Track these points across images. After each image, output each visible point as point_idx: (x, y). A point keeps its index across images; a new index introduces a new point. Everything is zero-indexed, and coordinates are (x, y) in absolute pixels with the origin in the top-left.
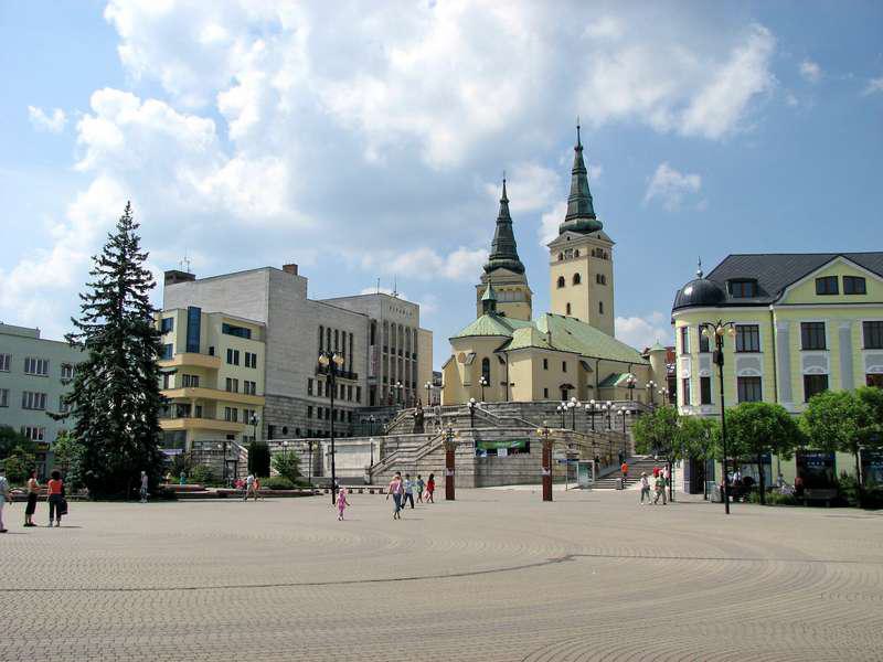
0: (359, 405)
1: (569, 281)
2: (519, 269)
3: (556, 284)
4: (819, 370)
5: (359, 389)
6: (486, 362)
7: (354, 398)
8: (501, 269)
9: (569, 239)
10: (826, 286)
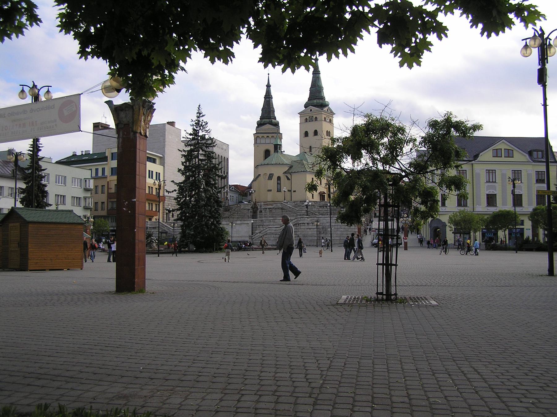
1: (311, 133)
2: (277, 125)
3: (303, 135)
4: (493, 192)
6: (279, 178)
8: (268, 124)
9: (311, 110)
10: (497, 153)
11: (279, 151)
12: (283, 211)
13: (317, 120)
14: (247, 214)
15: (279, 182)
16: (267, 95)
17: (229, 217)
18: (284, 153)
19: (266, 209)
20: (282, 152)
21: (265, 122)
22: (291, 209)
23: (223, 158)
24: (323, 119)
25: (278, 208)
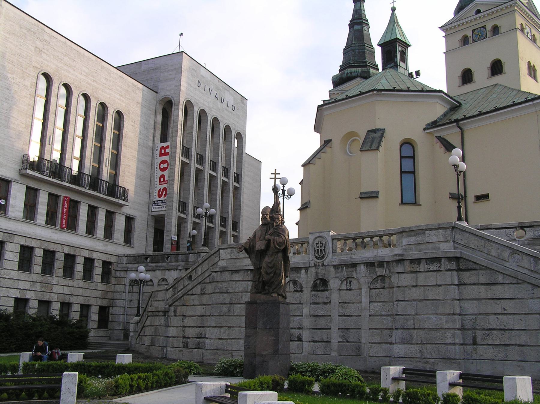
0: (128, 251)
3: (458, 81)
5: (129, 220)
7: (100, 231)
11: (402, 64)
13: (498, 33)
15: (408, 165)
16: (356, 17)
17: (165, 312)
18: (419, 79)
19: (354, 265)
20: (411, 75)
21: (351, 73)
23: (222, 127)
24: (518, 26)
25: (432, 260)
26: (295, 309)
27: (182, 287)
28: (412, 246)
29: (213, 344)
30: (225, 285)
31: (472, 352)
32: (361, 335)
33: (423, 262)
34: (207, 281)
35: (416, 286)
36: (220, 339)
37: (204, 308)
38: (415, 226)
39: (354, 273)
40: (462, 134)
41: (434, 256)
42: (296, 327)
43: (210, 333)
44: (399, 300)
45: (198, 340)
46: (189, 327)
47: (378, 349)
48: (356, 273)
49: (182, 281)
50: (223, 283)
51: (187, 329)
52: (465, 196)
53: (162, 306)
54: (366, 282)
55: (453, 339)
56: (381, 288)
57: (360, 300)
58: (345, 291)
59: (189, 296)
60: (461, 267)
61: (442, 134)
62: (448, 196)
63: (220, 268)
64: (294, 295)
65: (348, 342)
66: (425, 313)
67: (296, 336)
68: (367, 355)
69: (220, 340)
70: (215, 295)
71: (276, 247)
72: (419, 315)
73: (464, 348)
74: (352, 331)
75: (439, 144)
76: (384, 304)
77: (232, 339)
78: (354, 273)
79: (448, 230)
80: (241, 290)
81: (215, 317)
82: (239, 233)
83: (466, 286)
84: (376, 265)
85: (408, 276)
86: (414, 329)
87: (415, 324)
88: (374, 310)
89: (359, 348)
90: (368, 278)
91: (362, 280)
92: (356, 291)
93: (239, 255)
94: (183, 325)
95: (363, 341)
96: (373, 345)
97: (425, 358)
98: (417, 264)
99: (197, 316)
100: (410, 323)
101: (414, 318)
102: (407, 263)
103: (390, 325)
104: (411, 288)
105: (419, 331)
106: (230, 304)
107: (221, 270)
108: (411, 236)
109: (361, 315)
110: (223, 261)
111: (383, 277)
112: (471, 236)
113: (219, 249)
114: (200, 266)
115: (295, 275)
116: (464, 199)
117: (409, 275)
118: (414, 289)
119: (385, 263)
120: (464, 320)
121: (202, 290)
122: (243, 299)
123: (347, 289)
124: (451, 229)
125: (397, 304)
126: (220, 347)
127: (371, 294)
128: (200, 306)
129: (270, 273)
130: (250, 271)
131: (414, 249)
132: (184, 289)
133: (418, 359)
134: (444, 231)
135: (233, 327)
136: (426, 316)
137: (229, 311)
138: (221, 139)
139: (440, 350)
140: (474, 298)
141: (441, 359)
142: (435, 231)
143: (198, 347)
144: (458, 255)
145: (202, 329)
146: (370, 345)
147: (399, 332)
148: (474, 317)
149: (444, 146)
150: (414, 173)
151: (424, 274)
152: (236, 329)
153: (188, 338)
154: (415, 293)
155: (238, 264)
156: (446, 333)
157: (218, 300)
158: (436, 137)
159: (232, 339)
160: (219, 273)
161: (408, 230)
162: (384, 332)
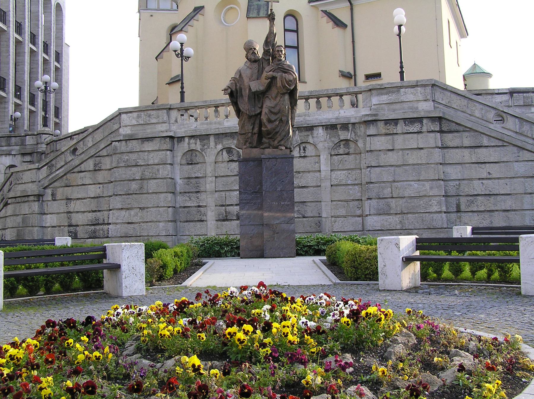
12: (451, 139)
14: (165, 171)
17: (39, 197)
22: (511, 123)
26: (232, 182)
27: (63, 163)
28: (383, 106)
29: (119, 230)
30: (133, 156)
31: (456, 220)
32: (321, 209)
33: (401, 123)
34: (104, 153)
35: (393, 150)
36: (129, 223)
37: (100, 188)
38: (388, 84)
39: (310, 137)
40: (352, 9)
41: (415, 116)
42: (234, 203)
43: (115, 217)
44: (371, 166)
45: (93, 227)
46: (78, 212)
47: (344, 223)
48: (313, 137)
49: (63, 156)
50: (130, 155)
51: (73, 215)
52: (355, 75)
53: (33, 189)
54: (325, 148)
55: (439, 207)
56: (344, 154)
57: (319, 168)
58: (297, 159)
59: (75, 174)
60: (443, 129)
61: (328, 8)
62: (337, 74)
63: (125, 136)
64: (229, 165)
65: (304, 217)
66: (404, 179)
67: (235, 214)
68: (329, 231)
69: (130, 225)
70: (120, 169)
71: (284, 87)
72: (398, 182)
73: (447, 217)
74: (309, 204)
75: (326, 18)
76: (350, 172)
77: (147, 222)
78: (310, 137)
79: (428, 88)
80: (156, 162)
81: (120, 196)
82: (61, 120)
83: (449, 150)
84: (339, 128)
85: (383, 138)
86: (392, 197)
87: (393, 193)
88: (338, 179)
89: (319, 224)
90: (328, 143)
91: (320, 146)
92: (312, 158)
93: (149, 121)
94: (68, 211)
95: (324, 215)
96: (338, 219)
97: (406, 229)
98: (394, 126)
99: (89, 198)
100: (387, 192)
101: (392, 185)
102: (381, 125)
103: (358, 196)
104: (388, 152)
105: (398, 199)
106: (141, 179)
107: (127, 139)
108: (382, 94)
109: (320, 186)
110: (125, 129)
111: (347, 140)
112: (453, 95)
113: (120, 114)
114: (91, 136)
115: (230, 142)
116: (353, 77)
117: (383, 137)
118: (390, 153)
119: (350, 125)
120: (446, 186)
121: (95, 165)
122: (161, 172)
123: (300, 157)
124: (430, 87)
125: (370, 171)
126: (131, 233)
127: (332, 161)
128: (94, 186)
129: (275, 120)
130: (168, 138)
131: (386, 109)
132: (66, 166)
133: (398, 231)
134: (423, 88)
135: (148, 208)
136: (405, 183)
137: (141, 188)
138: (40, 7)
139: (424, 219)
140: (457, 162)
141: (425, 229)
142: (412, 89)
143: (93, 236)
144: (441, 115)
145: (98, 213)
146: (333, 219)
147: (374, 202)
148: (457, 183)
149: (332, 20)
150: (297, 48)
151: (402, 136)
152: (151, 209)
153: (77, 226)
154: (392, 158)
155: (149, 131)
156: (431, 201)
157: (124, 176)
158: (322, 11)
159: (147, 222)
160: (124, 142)
161: (379, 87)
162: (351, 203)
